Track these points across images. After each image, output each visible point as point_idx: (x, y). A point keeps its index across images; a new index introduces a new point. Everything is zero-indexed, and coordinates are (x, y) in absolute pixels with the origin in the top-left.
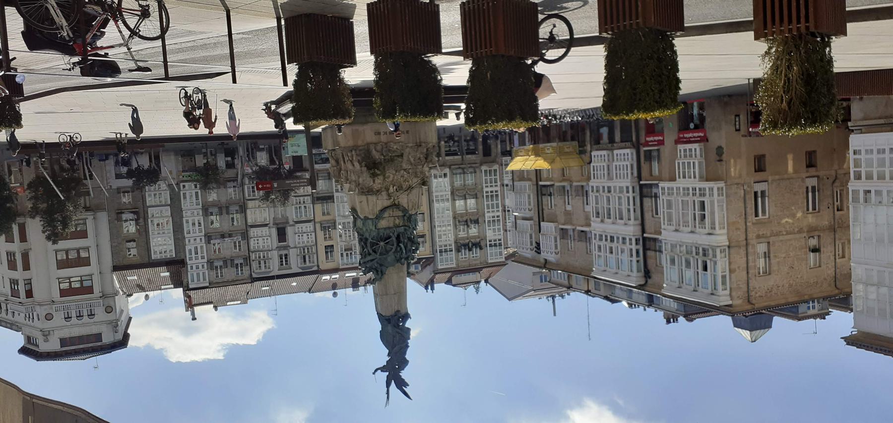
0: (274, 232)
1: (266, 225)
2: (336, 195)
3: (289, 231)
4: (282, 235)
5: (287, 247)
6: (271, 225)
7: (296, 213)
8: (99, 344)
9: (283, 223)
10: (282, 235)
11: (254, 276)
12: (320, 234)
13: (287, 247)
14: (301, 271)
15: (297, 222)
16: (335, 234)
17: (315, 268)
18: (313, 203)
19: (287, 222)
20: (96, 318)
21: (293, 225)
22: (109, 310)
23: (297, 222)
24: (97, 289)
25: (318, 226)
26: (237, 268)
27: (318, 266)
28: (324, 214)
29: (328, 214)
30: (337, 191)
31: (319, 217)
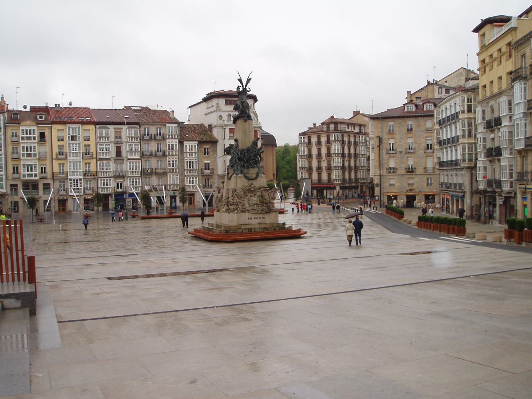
0: (124, 154)
1: (129, 159)
2: (82, 177)
3: (114, 154)
4: (119, 152)
5: (116, 143)
6: (125, 159)
7: (109, 166)
8: (227, 99)
9: (118, 159)
10: (119, 152)
11: (138, 126)
12: (92, 149)
13: (116, 143)
14: (108, 126)
15: (109, 159)
16: (82, 150)
17: (98, 126)
18: (97, 172)
19: (115, 160)
20: (227, 114)
21: (111, 157)
22: (220, 117)
23: (109, 159)
24: (227, 131)
25: (94, 156)
26: (148, 133)
27: (96, 128)
28: (89, 163)
29: (86, 164)
30: (80, 179)
31: (93, 162)
